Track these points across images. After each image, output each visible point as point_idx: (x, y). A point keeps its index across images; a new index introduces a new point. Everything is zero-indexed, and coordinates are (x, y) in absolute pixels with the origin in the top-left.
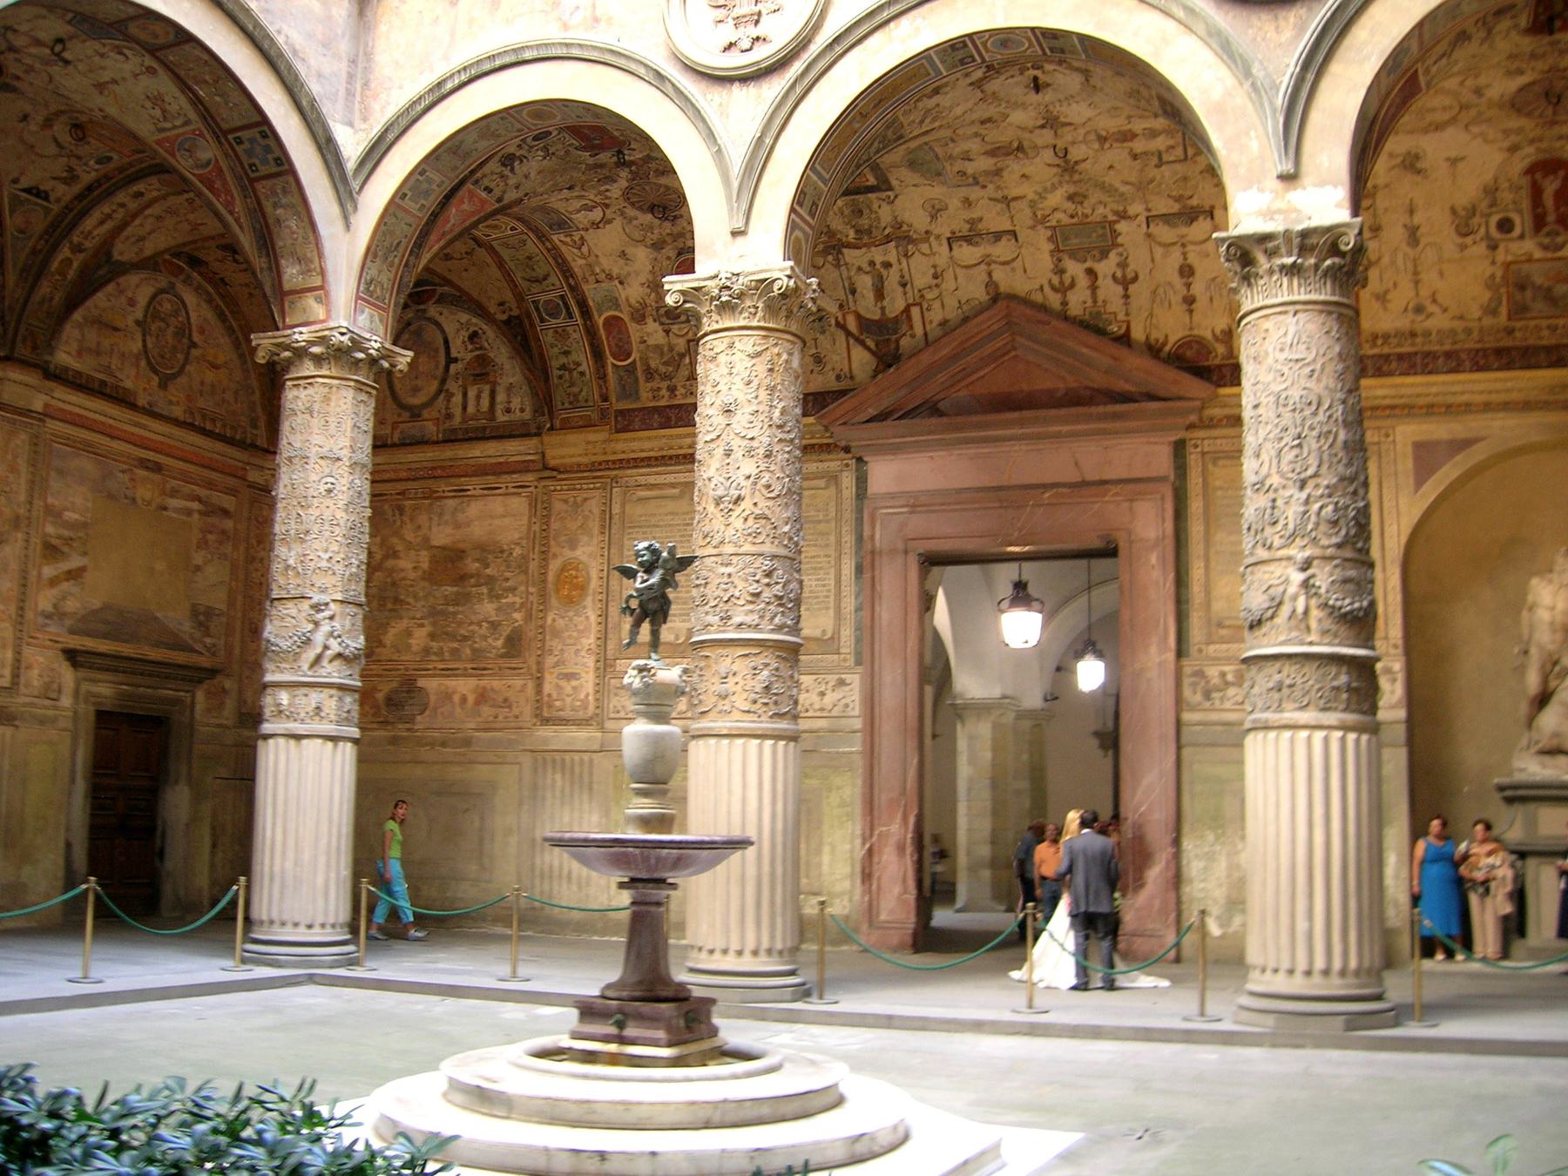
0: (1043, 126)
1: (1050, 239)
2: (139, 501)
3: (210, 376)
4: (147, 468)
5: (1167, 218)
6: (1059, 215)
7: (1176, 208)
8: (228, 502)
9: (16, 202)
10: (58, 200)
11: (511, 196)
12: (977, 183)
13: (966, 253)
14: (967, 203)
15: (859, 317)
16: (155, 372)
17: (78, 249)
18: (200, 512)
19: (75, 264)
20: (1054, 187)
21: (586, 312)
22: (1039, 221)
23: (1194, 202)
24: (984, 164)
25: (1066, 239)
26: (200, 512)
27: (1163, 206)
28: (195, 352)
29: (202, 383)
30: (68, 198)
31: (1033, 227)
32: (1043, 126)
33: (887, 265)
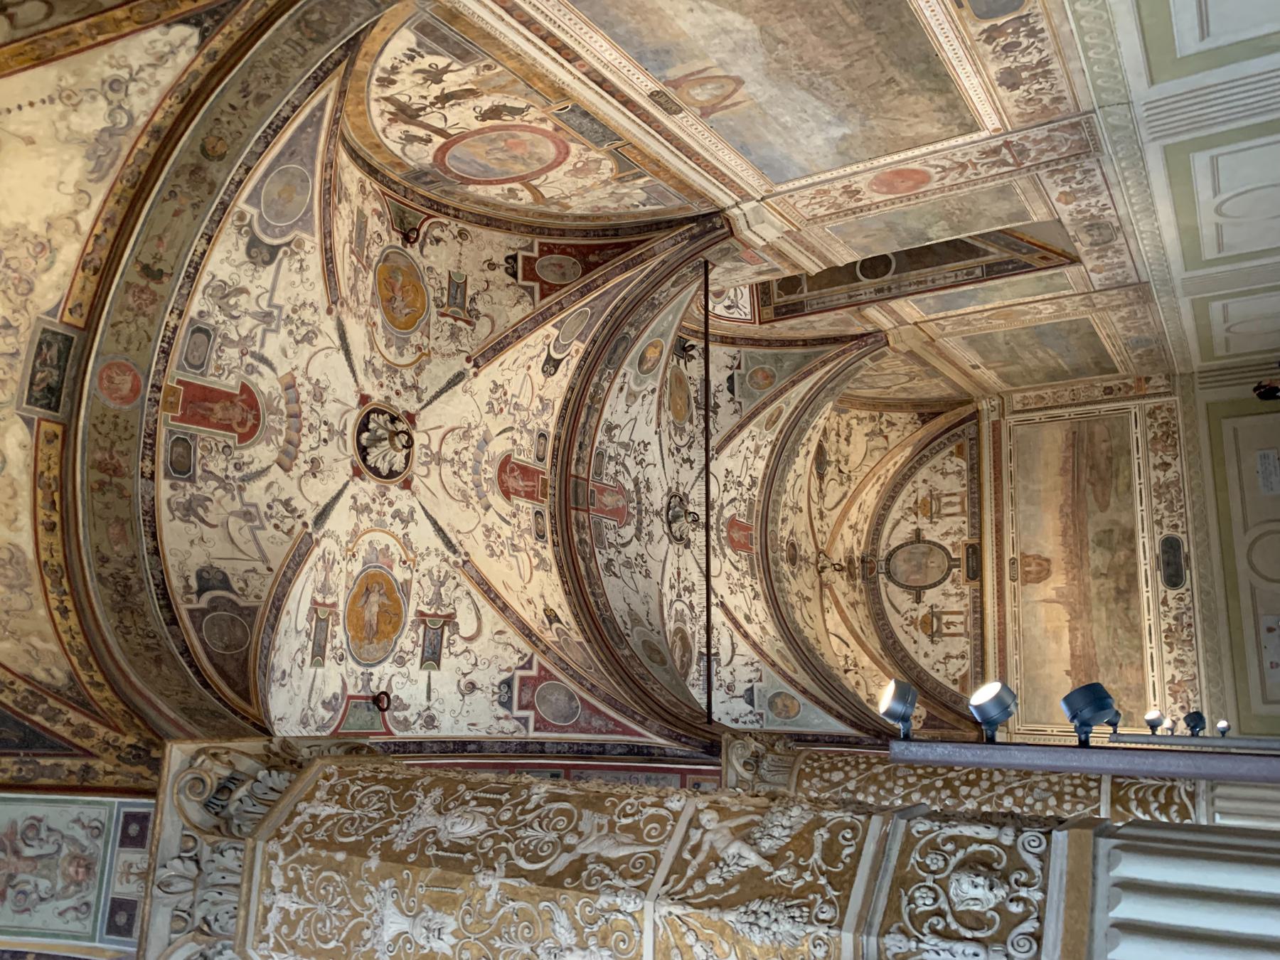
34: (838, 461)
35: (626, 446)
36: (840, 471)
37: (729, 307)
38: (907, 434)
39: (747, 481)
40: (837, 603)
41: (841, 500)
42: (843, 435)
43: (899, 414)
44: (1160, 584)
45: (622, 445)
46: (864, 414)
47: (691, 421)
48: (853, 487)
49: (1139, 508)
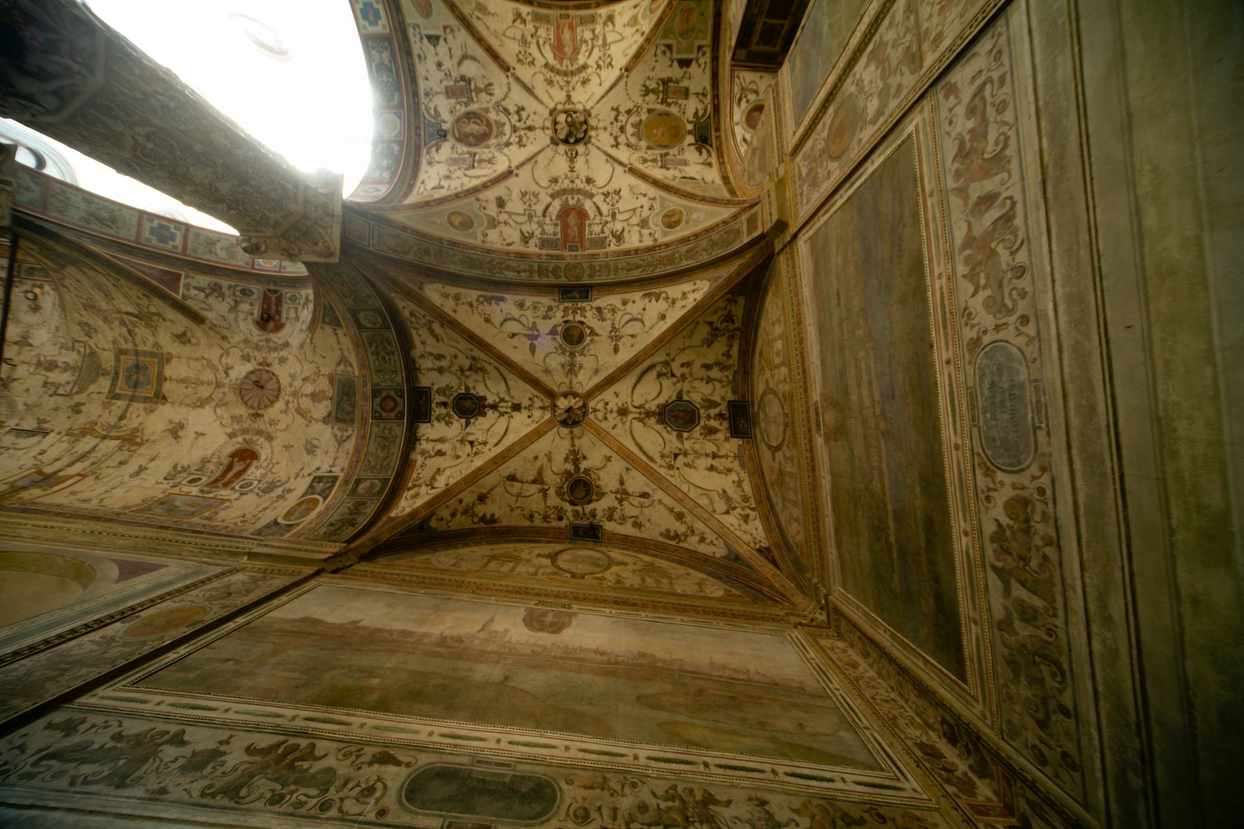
23: (45, 426)
34: (686, 454)
35: (605, 44)
36: (676, 456)
37: (745, 140)
38: (738, 533)
39: (618, 226)
40: (538, 434)
41: (645, 453)
42: (716, 463)
43: (760, 528)
44: (434, 758)
45: (605, 39)
46: (747, 487)
47: (649, 148)
48: (662, 471)
49: (643, 754)
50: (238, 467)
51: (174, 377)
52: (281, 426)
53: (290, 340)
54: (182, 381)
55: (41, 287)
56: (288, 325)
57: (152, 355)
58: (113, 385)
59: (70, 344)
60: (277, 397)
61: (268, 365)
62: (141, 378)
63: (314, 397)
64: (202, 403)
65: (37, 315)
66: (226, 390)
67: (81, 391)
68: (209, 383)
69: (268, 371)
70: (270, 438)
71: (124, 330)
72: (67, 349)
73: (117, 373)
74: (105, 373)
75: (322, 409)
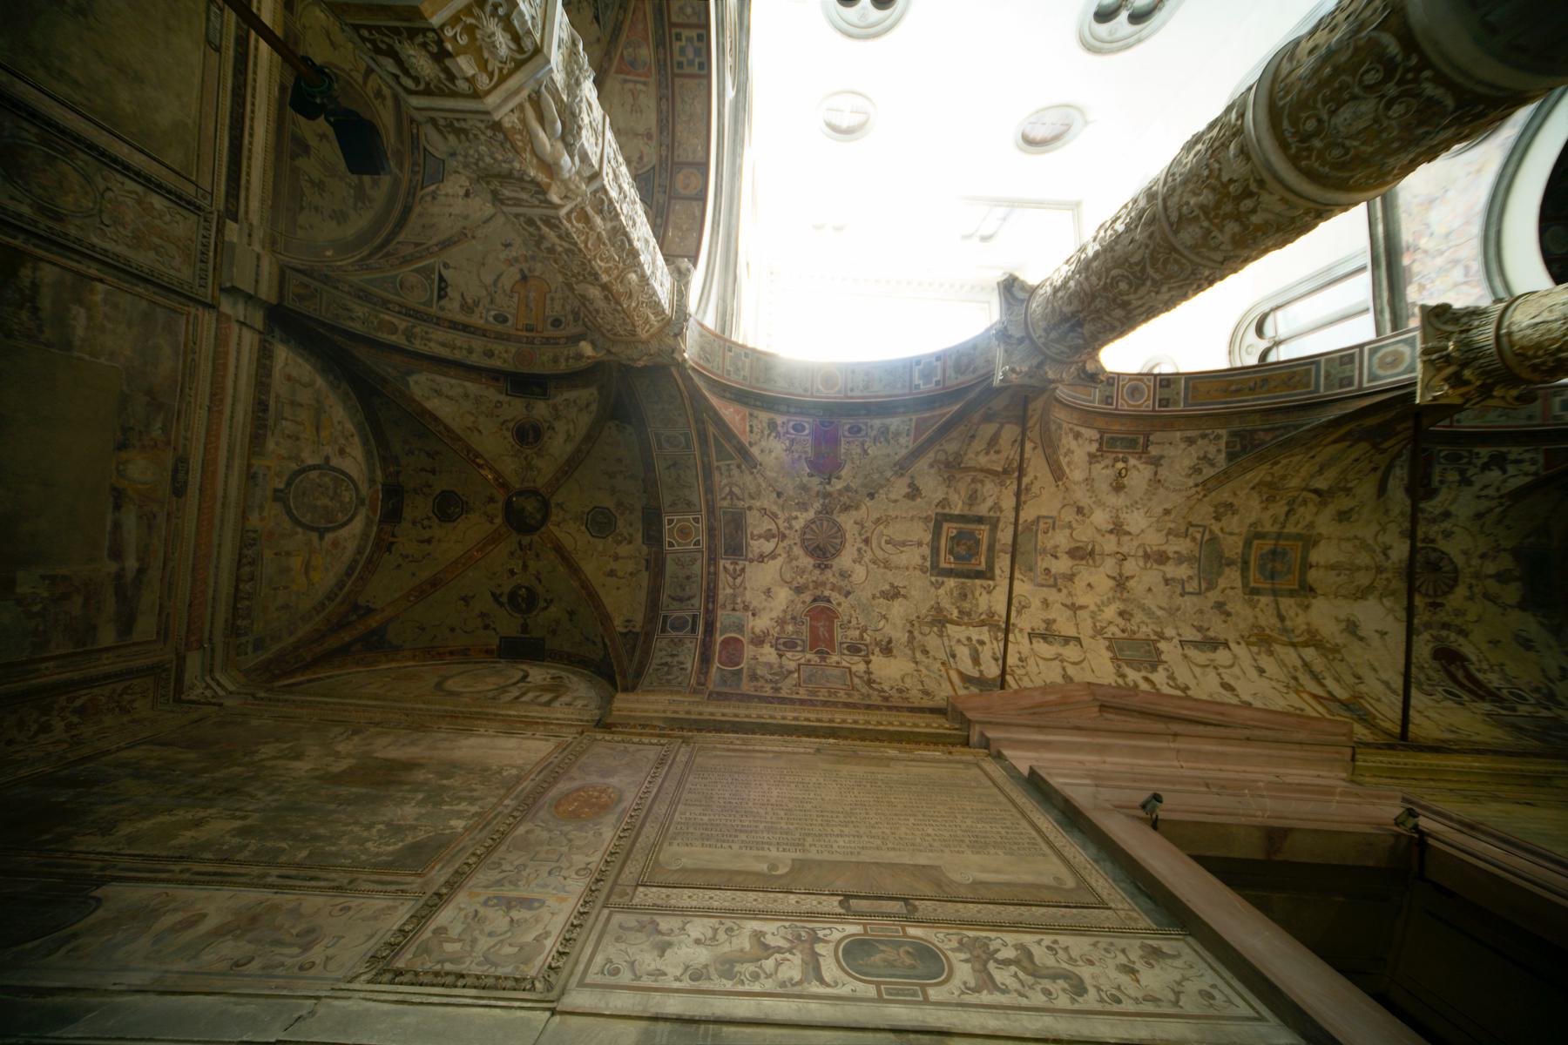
0: (1111, 532)
1: (1109, 648)
2: (124, 455)
3: (296, 563)
4: (175, 471)
5: (1196, 644)
6: (1113, 629)
7: (1198, 637)
8: (146, 625)
9: (426, 272)
10: (442, 309)
11: (755, 451)
12: (1055, 585)
13: (1042, 648)
14: (1046, 603)
15: (960, 673)
16: (288, 484)
17: (409, 335)
18: (119, 576)
19: (393, 338)
20: (1110, 601)
21: (710, 628)
22: (1099, 632)
23: (1211, 634)
24: (1062, 565)
25: (1121, 650)
26: (119, 576)
27: (1191, 634)
28: (315, 536)
29: (288, 554)
30: (449, 315)
31: (1093, 637)
32: (1111, 532)
33: (982, 643)
50: (1460, 675)
51: (1322, 562)
52: (1471, 617)
53: (1453, 509)
54: (1332, 567)
55: (1125, 461)
56: (1444, 490)
57: (1299, 537)
58: (1244, 577)
59: (1183, 530)
60: (1456, 580)
61: (1433, 541)
62: (1278, 566)
63: (1500, 577)
64: (1362, 594)
65: (1122, 494)
66: (1389, 575)
67: (1211, 586)
68: (1367, 568)
69: (1434, 550)
70: (1462, 632)
71: (1286, 508)
72: (1177, 536)
73: (1246, 563)
74: (1230, 563)
75: (1512, 593)
